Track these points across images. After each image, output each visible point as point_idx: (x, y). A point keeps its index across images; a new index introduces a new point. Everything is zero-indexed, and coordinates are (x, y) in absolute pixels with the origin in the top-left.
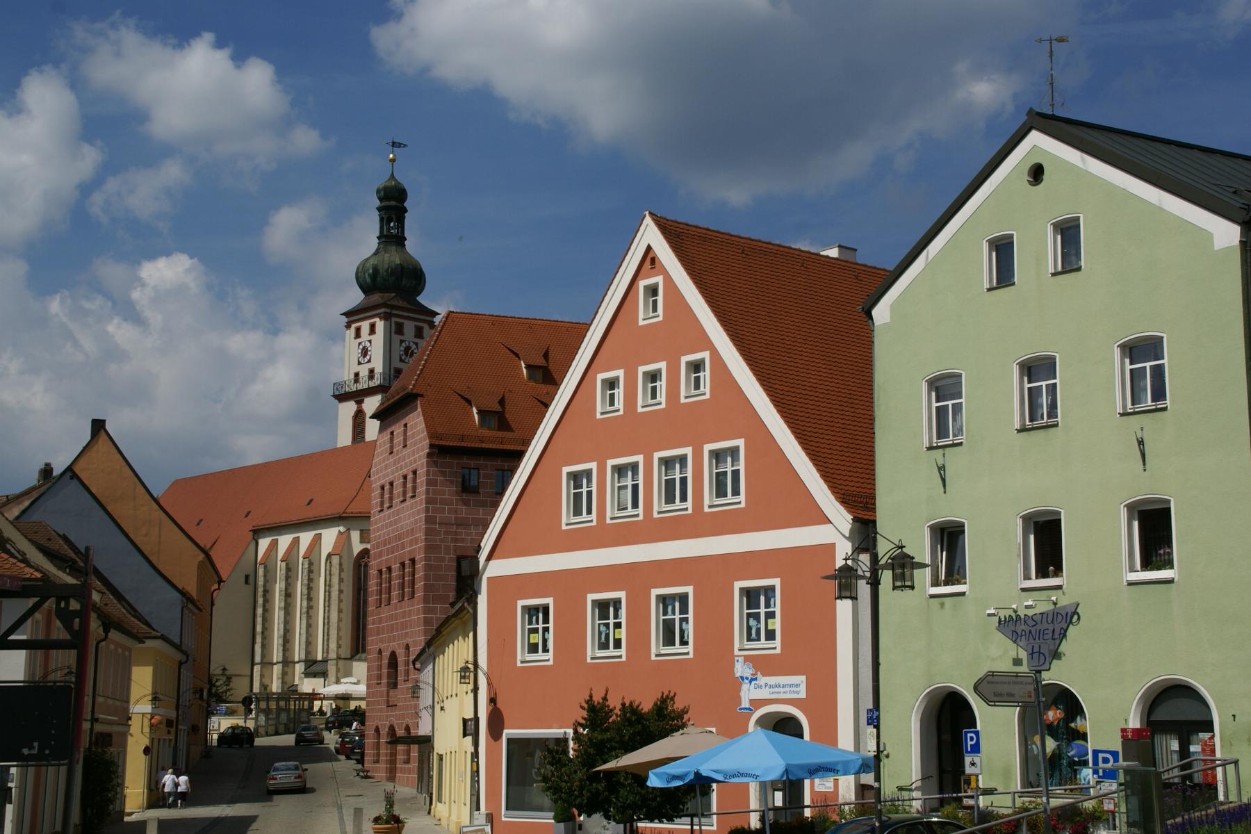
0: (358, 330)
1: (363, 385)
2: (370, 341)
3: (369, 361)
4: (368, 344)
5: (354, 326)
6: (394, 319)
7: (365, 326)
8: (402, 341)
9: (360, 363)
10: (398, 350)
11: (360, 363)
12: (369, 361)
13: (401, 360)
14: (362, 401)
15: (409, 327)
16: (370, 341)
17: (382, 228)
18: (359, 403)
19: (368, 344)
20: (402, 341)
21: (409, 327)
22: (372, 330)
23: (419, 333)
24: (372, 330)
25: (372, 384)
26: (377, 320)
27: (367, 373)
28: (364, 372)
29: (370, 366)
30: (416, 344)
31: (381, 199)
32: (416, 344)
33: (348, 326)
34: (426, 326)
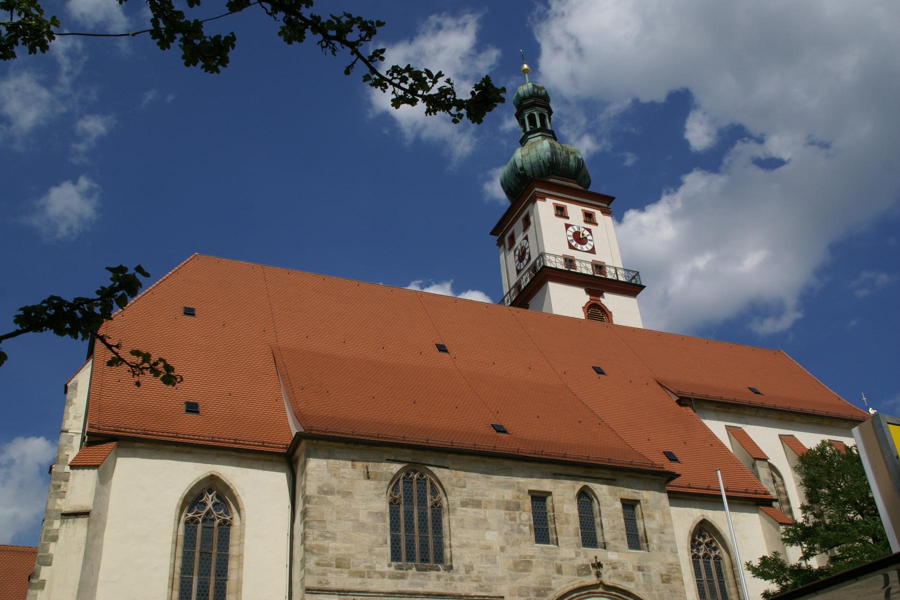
2: (526, 238)
8: (567, 226)
13: (571, 247)
20: (567, 226)
30: (589, 230)
32: (589, 230)
34: (598, 214)
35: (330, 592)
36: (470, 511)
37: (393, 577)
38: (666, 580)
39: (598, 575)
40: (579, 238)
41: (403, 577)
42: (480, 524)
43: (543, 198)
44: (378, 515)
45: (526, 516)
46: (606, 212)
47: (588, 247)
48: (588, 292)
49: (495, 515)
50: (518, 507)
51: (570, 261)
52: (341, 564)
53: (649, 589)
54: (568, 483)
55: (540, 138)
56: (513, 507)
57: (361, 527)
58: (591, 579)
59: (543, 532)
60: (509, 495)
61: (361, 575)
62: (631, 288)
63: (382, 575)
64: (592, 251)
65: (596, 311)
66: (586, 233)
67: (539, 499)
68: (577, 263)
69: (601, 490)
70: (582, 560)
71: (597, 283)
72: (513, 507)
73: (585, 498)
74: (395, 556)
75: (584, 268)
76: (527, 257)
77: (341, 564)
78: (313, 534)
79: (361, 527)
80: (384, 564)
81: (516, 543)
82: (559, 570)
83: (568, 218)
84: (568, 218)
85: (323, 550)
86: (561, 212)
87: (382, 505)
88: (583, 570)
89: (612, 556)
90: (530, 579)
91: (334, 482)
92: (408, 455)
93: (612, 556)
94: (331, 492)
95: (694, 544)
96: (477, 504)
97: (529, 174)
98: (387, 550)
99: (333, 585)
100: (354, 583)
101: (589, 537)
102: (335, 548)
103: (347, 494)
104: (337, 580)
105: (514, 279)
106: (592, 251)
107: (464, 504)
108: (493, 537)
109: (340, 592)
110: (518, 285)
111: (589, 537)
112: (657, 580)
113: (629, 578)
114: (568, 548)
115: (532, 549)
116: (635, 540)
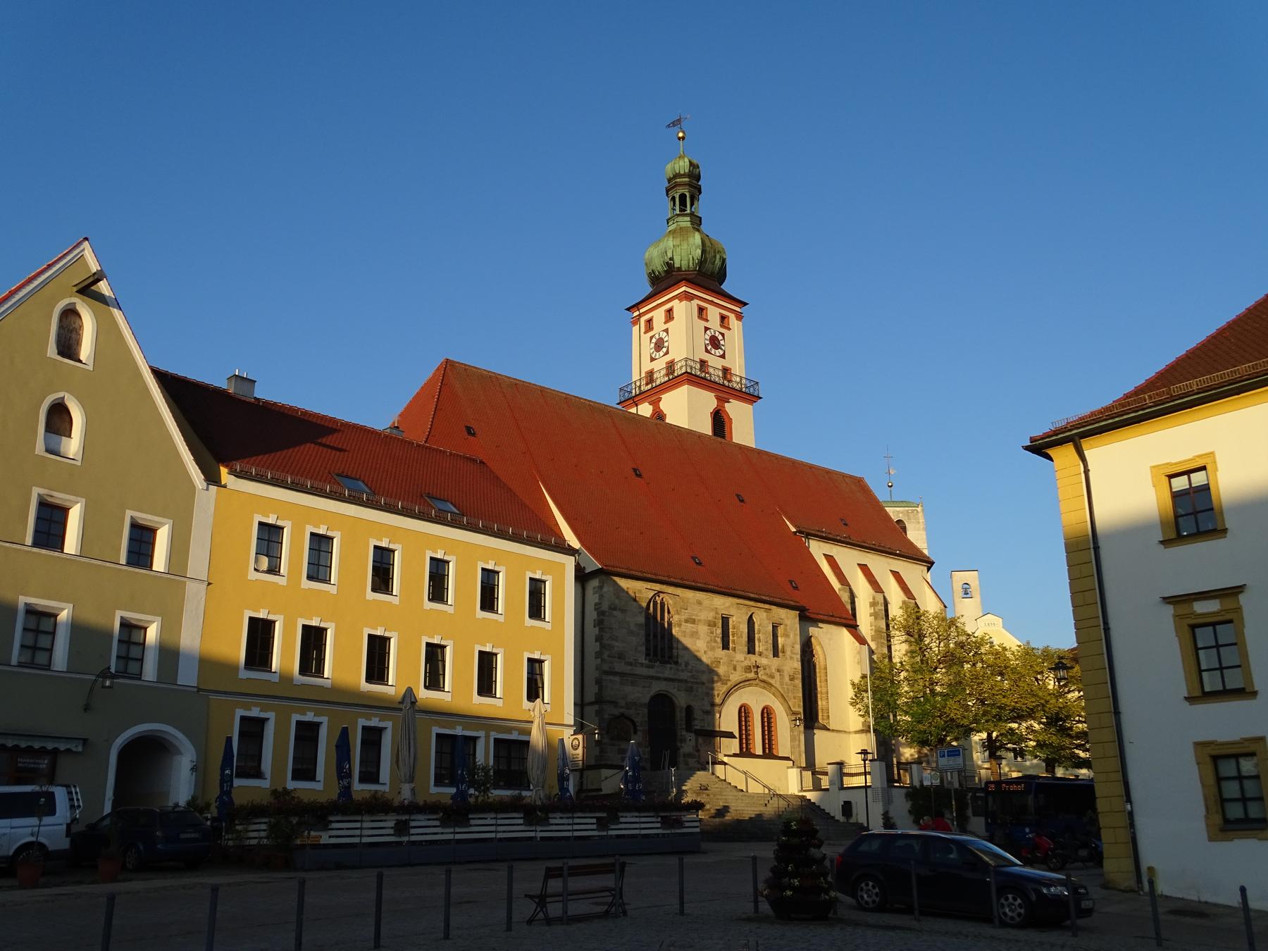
0: (650, 321)
2: (666, 331)
3: (667, 353)
4: (663, 335)
5: (643, 319)
6: (696, 302)
9: (652, 359)
10: (702, 339)
11: (652, 359)
12: (667, 353)
13: (707, 351)
14: (660, 399)
15: (714, 313)
16: (666, 331)
18: (655, 403)
19: (663, 335)
20: (706, 329)
21: (714, 313)
22: (669, 315)
24: (669, 315)
28: (660, 365)
29: (668, 358)
30: (723, 335)
32: (723, 335)
33: (636, 321)
34: (732, 317)
35: (615, 674)
36: (689, 625)
37: (648, 667)
38: (792, 679)
39: (757, 673)
40: (714, 342)
41: (652, 667)
45: (719, 631)
46: (739, 317)
47: (719, 352)
48: (718, 398)
49: (703, 629)
50: (715, 625)
51: (703, 363)
52: (621, 656)
53: (782, 684)
54: (744, 609)
56: (711, 624)
58: (752, 675)
61: (630, 664)
62: (750, 397)
63: (642, 665)
64: (723, 356)
65: (720, 421)
66: (720, 337)
70: (747, 663)
71: (724, 389)
72: (711, 624)
74: (647, 655)
75: (716, 375)
80: (642, 660)
81: (713, 649)
82: (735, 669)
83: (707, 320)
84: (707, 320)
88: (748, 669)
91: (617, 601)
92: (658, 587)
94: (615, 609)
96: (693, 622)
97: (677, 265)
98: (644, 649)
100: (627, 669)
101: (751, 650)
103: (623, 611)
104: (620, 667)
105: (647, 366)
106: (723, 356)
107: (686, 621)
109: (622, 674)
110: (650, 374)
111: (751, 650)
112: (787, 679)
114: (740, 656)
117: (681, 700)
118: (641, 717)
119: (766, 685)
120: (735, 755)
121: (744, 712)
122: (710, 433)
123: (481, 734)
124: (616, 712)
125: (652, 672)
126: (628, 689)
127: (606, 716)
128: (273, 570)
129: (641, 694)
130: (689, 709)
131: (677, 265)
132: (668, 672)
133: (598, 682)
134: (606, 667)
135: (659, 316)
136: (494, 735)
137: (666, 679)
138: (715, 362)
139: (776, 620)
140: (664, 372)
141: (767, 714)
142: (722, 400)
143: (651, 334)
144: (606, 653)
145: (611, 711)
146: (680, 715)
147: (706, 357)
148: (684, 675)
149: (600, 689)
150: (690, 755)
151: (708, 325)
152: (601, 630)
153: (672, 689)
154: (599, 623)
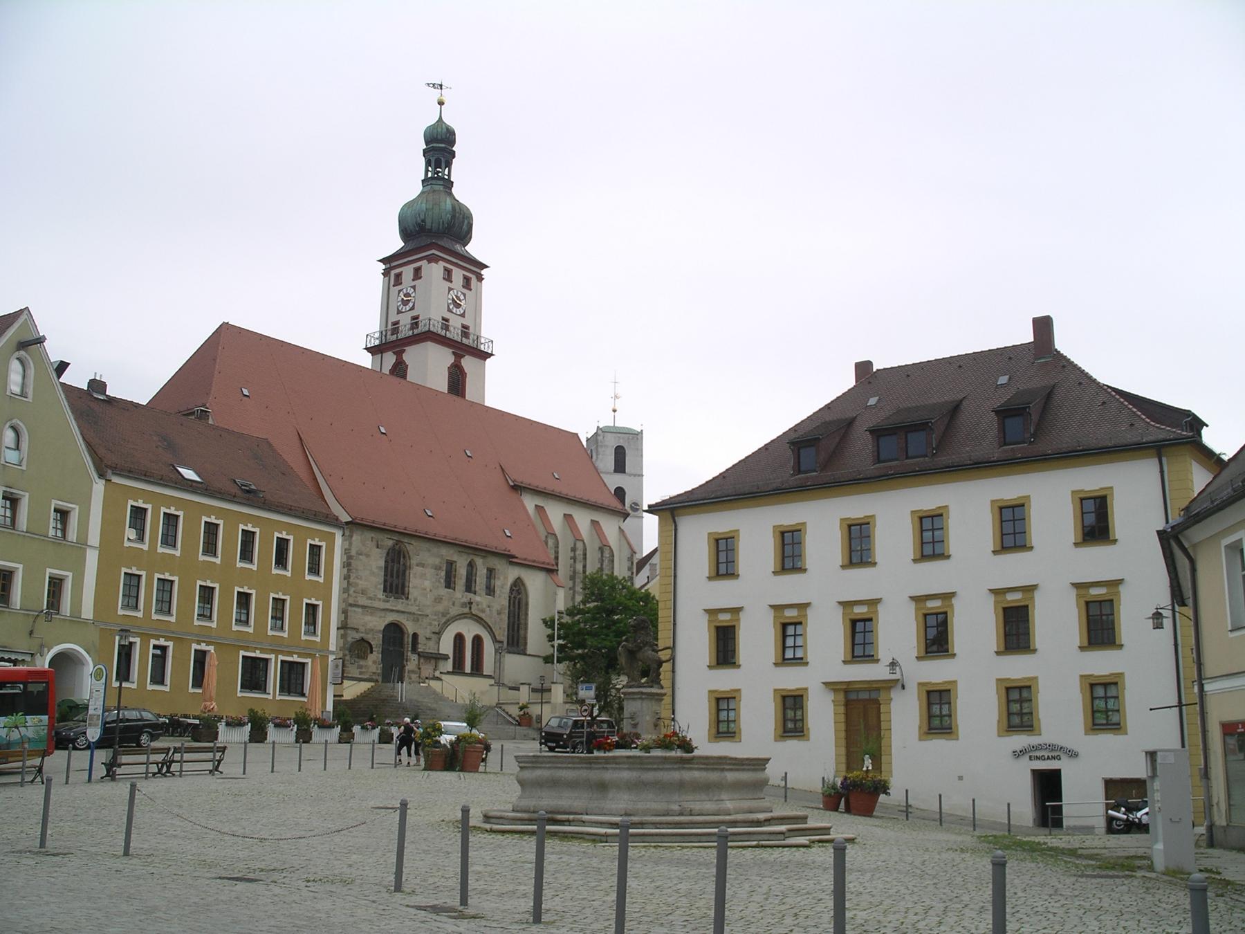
0: (398, 276)
1: (405, 331)
2: (414, 287)
3: (413, 308)
5: (393, 272)
6: (442, 264)
7: (407, 272)
8: (450, 289)
9: (399, 312)
11: (399, 312)
13: (449, 310)
15: (458, 275)
16: (414, 287)
17: (427, 171)
18: (399, 354)
20: (450, 289)
21: (458, 275)
23: (467, 284)
24: (417, 274)
25: (416, 332)
26: (424, 263)
27: (409, 321)
28: (405, 320)
29: (413, 313)
31: (427, 143)
36: (420, 569)
38: (499, 613)
42: (423, 576)
43: (436, 262)
44: (379, 568)
45: (443, 574)
49: (430, 572)
52: (363, 592)
54: (465, 556)
55: (441, 188)
56: (438, 568)
57: (373, 574)
58: (466, 610)
59: (449, 583)
60: (437, 561)
61: (370, 598)
67: (450, 564)
68: (451, 329)
69: (479, 562)
70: (464, 600)
72: (438, 568)
73: (471, 565)
76: (411, 304)
77: (363, 592)
78: (353, 576)
79: (373, 574)
80: (381, 595)
85: (357, 585)
86: (448, 276)
87: (382, 563)
88: (464, 605)
89: (478, 598)
90: (440, 608)
93: (478, 598)
95: (511, 590)
96: (423, 566)
97: (428, 226)
99: (360, 603)
101: (469, 588)
102: (362, 584)
103: (368, 556)
104: (362, 601)
108: (427, 584)
109: (363, 607)
111: (469, 588)
112: (495, 613)
113: (483, 611)
114: (460, 594)
115: (444, 592)
116: (490, 591)
117: (410, 628)
118: (376, 641)
119: (479, 620)
120: (448, 673)
121: (459, 639)
122: (445, 389)
123: (272, 656)
124: (358, 636)
125: (388, 606)
126: (368, 618)
127: (349, 639)
128: (141, 538)
129: (378, 623)
130: (415, 636)
131: (428, 226)
132: (400, 605)
133: (345, 612)
134: (351, 601)
135: (407, 272)
136: (281, 657)
137: (398, 611)
138: (456, 323)
139: (491, 566)
140: (408, 327)
141: (477, 640)
142: (458, 357)
143: (399, 287)
144: (352, 590)
145: (353, 636)
146: (408, 640)
147: (448, 315)
148: (413, 609)
149: (346, 618)
150: (413, 672)
151: (451, 285)
152: (349, 570)
153: (401, 619)
154: (347, 565)
